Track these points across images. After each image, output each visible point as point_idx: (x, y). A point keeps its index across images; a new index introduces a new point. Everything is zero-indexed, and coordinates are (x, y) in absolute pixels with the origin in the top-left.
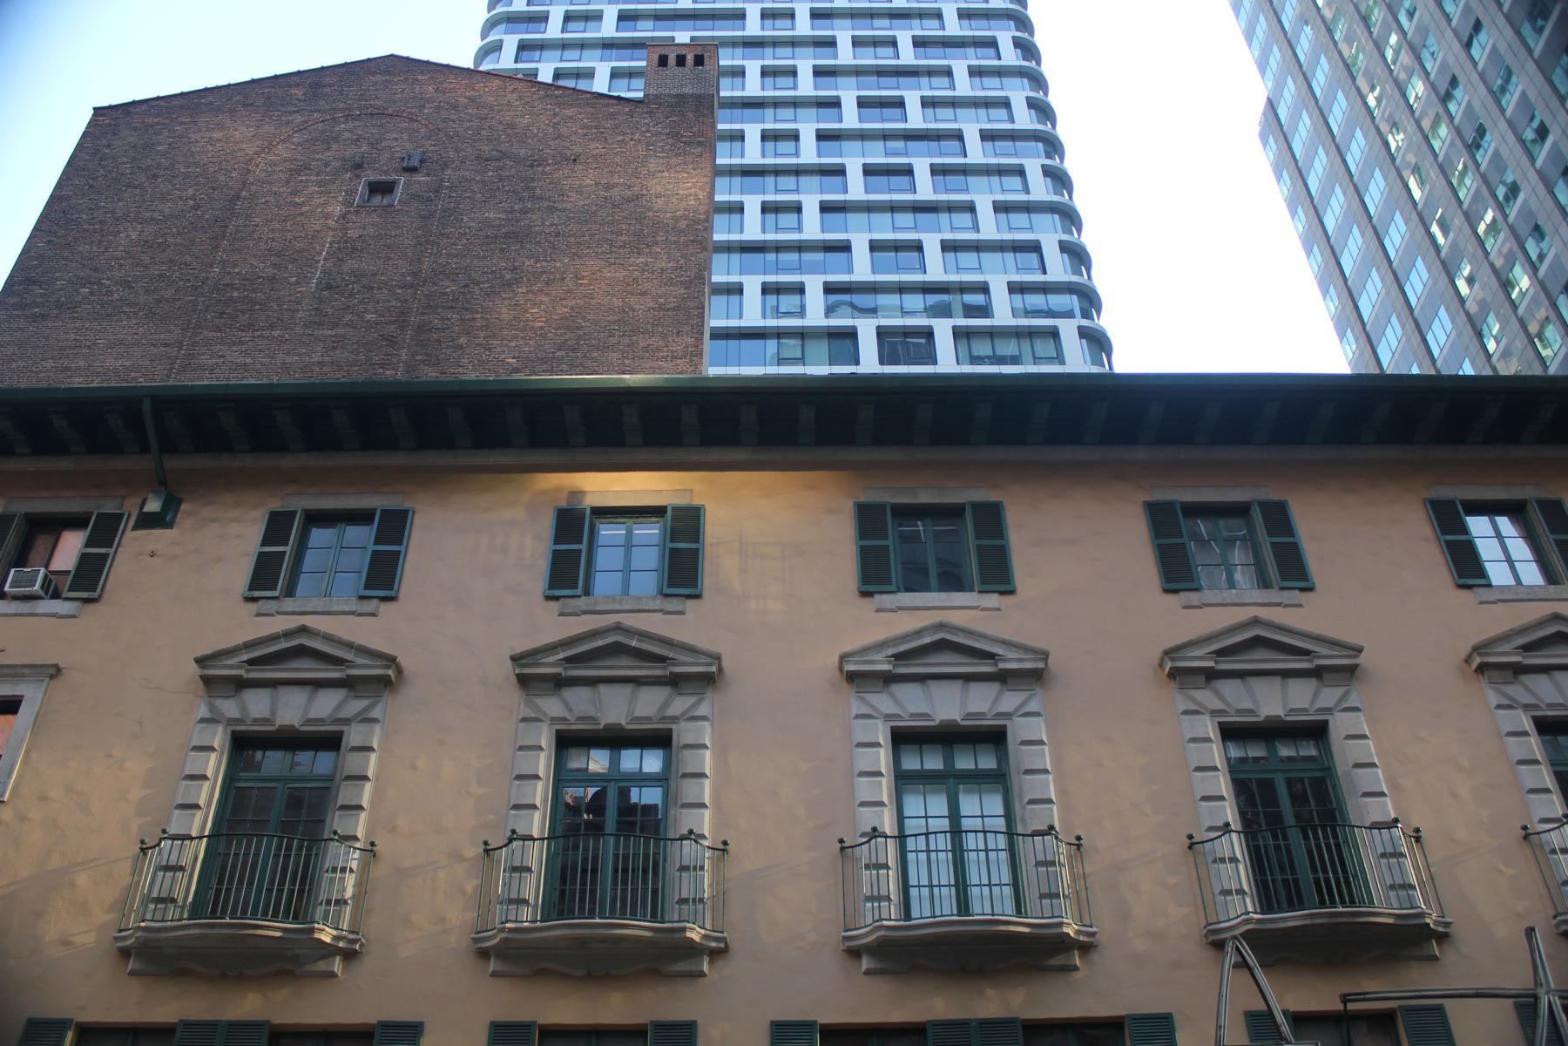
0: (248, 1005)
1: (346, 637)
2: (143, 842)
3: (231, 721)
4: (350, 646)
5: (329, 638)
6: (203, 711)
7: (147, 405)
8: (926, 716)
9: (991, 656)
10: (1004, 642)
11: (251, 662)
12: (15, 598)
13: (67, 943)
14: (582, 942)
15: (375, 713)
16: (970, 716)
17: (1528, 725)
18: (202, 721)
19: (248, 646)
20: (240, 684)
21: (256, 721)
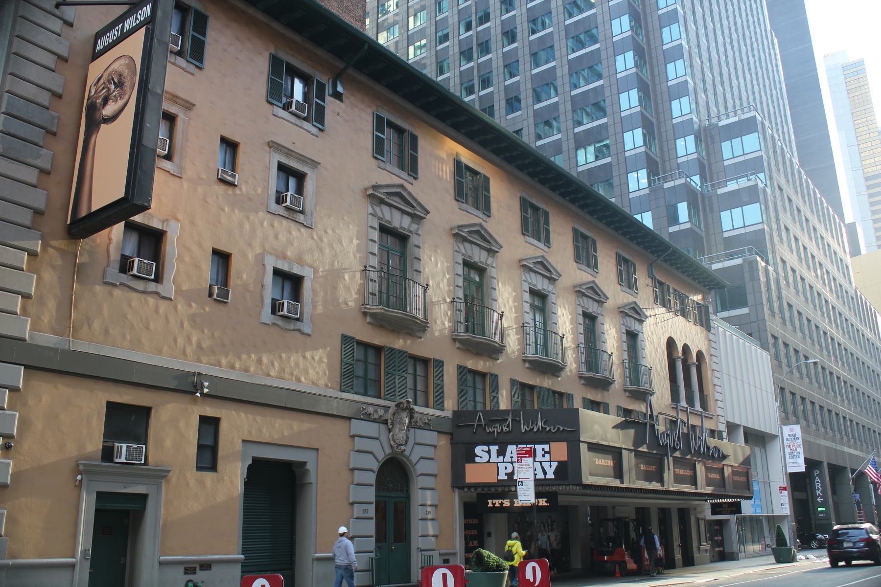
0: (400, 343)
1: (415, 196)
2: (365, 267)
3: (379, 218)
4: (416, 200)
5: (410, 194)
6: (370, 210)
7: (366, 47)
8: (535, 285)
9: (550, 271)
10: (554, 268)
11: (389, 194)
12: (292, 113)
13: (347, 304)
14: (836, 450)
15: (420, 232)
16: (544, 290)
17: (377, 226)
18: (371, 214)
19: (388, 186)
20: (382, 202)
21: (387, 221)
